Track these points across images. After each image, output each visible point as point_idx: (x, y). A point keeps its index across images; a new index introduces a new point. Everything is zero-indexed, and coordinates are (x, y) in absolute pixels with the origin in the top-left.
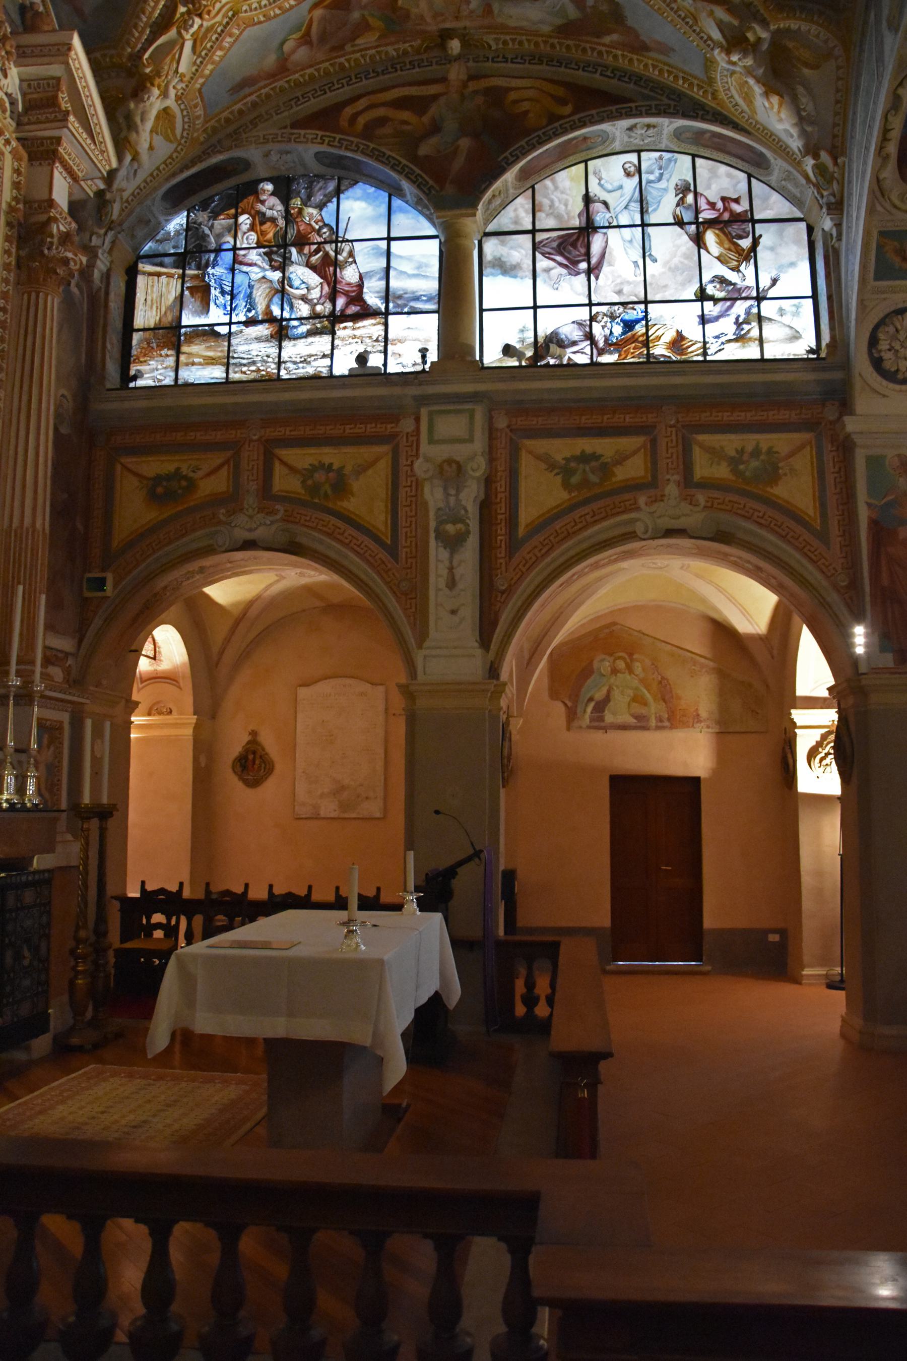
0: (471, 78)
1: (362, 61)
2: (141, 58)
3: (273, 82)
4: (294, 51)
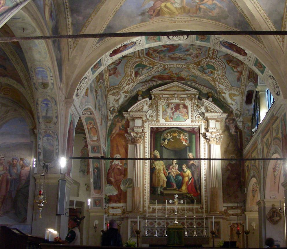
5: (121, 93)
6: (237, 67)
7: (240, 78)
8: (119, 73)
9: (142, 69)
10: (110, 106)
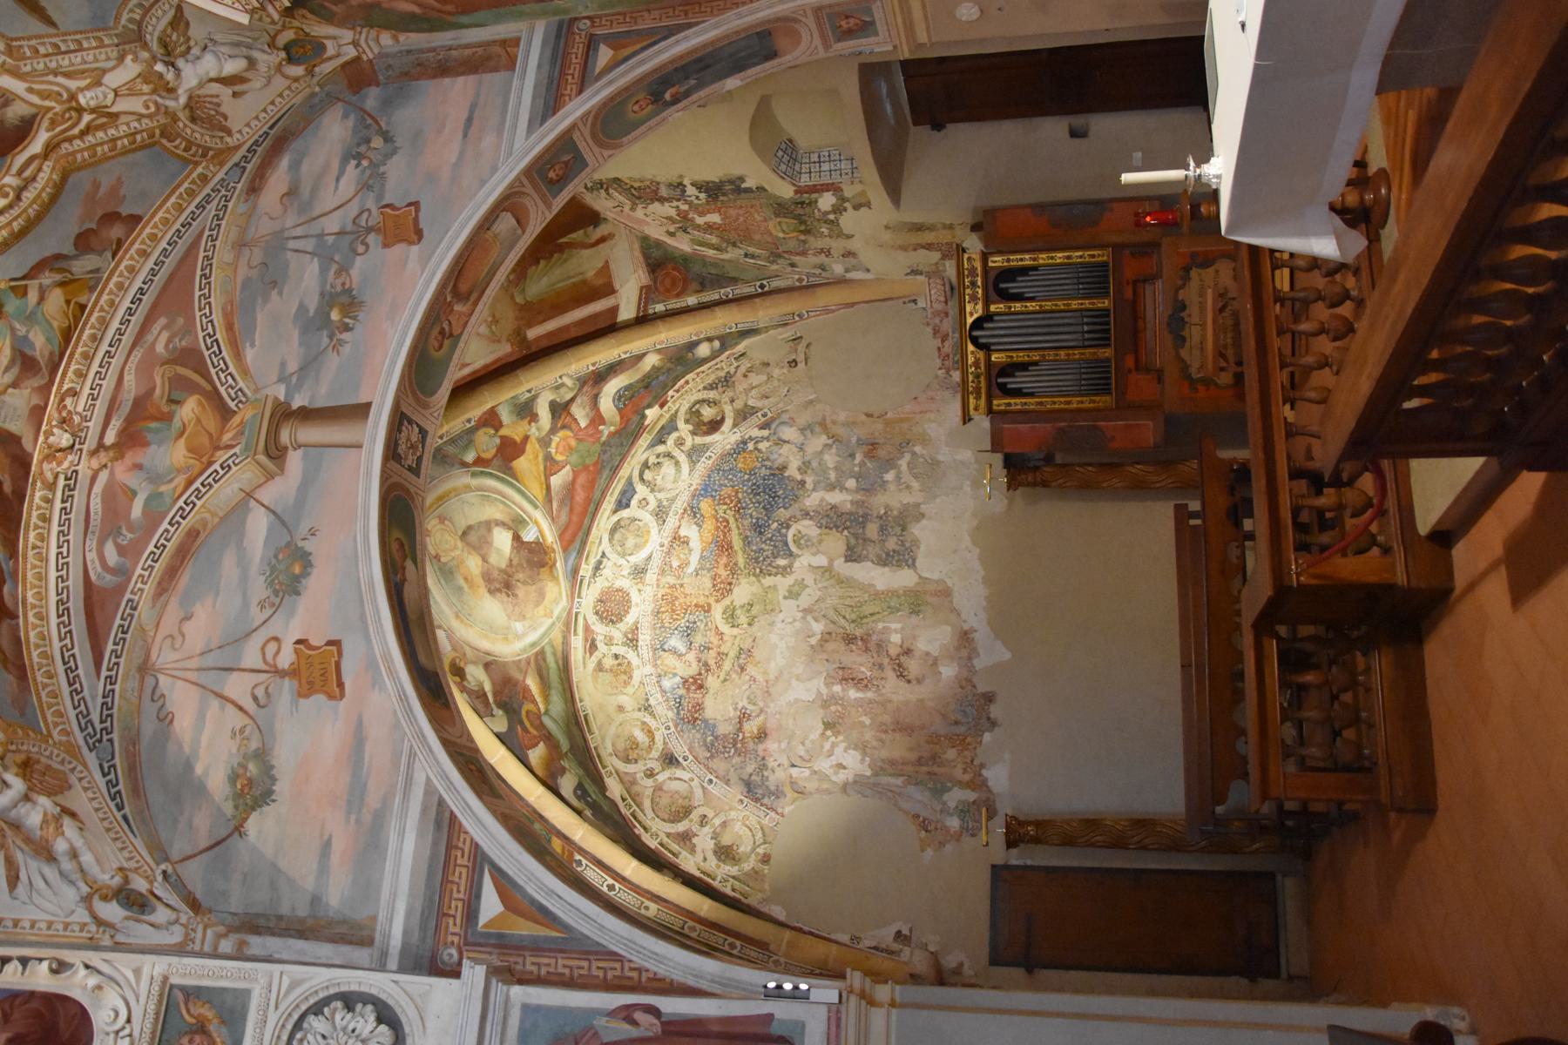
8: (91, 199)
10: (289, 88)
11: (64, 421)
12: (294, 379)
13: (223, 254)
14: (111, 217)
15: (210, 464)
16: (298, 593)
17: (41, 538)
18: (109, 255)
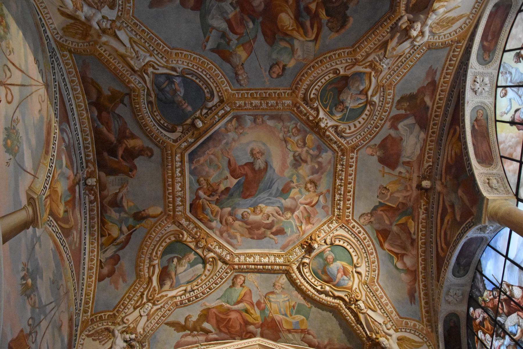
0: (441, 180)
1: (423, 232)
2: (369, 337)
3: (419, 280)
4: (404, 264)
5: (117, 330)
6: (403, 255)
7: (416, 292)
8: (123, 275)
9: (179, 260)
11: (92, 190)
12: (35, 242)
13: (70, 284)
14: (110, 274)
15: (50, 188)
16: (6, 129)
17: (86, 139)
18: (102, 260)
